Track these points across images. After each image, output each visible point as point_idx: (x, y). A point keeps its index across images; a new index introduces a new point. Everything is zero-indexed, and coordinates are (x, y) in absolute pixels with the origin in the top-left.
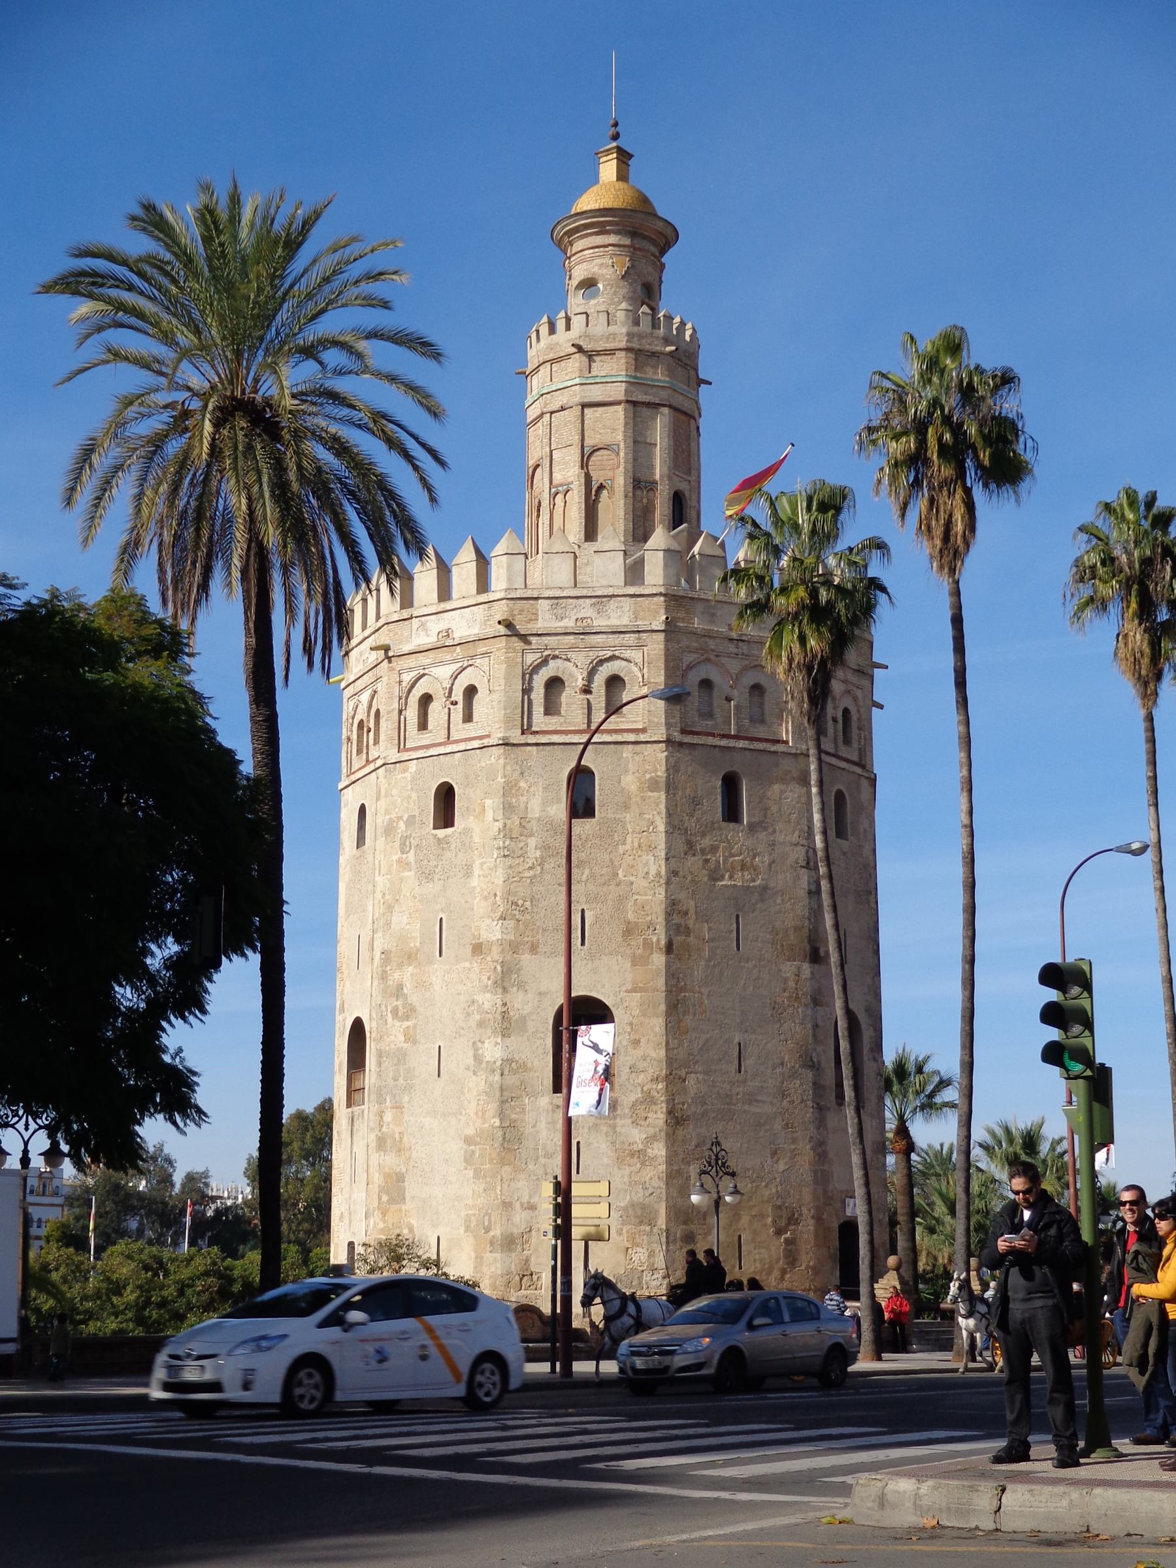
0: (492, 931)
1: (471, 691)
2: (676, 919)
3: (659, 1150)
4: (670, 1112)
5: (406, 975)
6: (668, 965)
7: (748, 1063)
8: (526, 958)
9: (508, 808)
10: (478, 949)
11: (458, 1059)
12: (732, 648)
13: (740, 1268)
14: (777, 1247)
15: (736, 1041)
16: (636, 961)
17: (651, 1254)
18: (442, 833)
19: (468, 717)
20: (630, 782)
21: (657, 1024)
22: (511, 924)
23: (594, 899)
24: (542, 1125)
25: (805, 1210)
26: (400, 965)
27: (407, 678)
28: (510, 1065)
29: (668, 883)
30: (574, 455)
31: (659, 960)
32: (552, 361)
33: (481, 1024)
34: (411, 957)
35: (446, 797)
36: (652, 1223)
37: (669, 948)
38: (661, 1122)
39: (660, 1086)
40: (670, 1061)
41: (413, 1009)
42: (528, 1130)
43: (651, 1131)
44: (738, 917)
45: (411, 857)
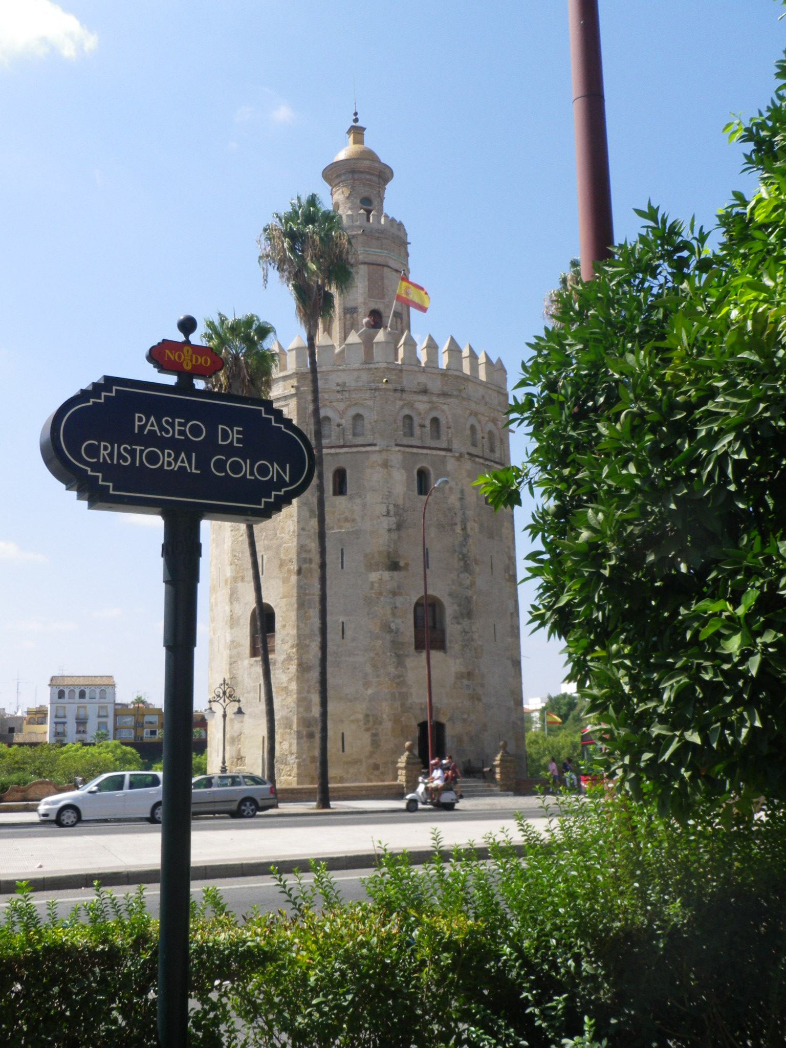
2: (304, 555)
3: (294, 686)
4: (300, 665)
6: (299, 581)
7: (348, 633)
8: (240, 585)
12: (339, 396)
13: (343, 751)
14: (367, 738)
15: (341, 621)
16: (286, 581)
17: (290, 746)
21: (293, 616)
22: (233, 566)
23: (268, 548)
24: (245, 676)
25: (385, 716)
28: (234, 645)
29: (299, 535)
31: (294, 578)
36: (291, 728)
37: (299, 572)
38: (294, 671)
39: (294, 650)
40: (299, 636)
42: (240, 679)
43: (290, 675)
44: (342, 550)
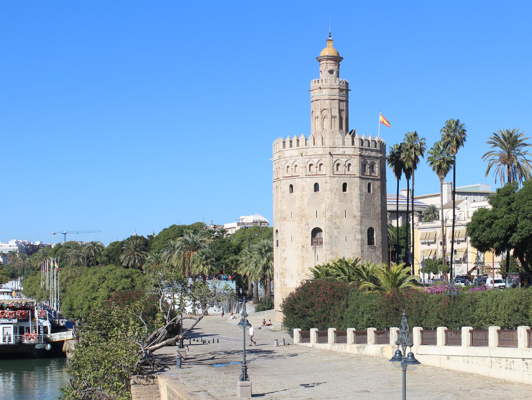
0: (358, 214)
1: (349, 165)
3: (381, 256)
5: (337, 221)
9: (360, 190)
10: (354, 217)
11: (350, 238)
16: (378, 221)
18: (345, 193)
19: (349, 170)
20: (376, 187)
26: (335, 219)
27: (334, 159)
30: (337, 110)
31: (380, 220)
32: (331, 88)
33: (356, 232)
34: (338, 217)
35: (345, 186)
41: (339, 227)
45: (337, 197)
